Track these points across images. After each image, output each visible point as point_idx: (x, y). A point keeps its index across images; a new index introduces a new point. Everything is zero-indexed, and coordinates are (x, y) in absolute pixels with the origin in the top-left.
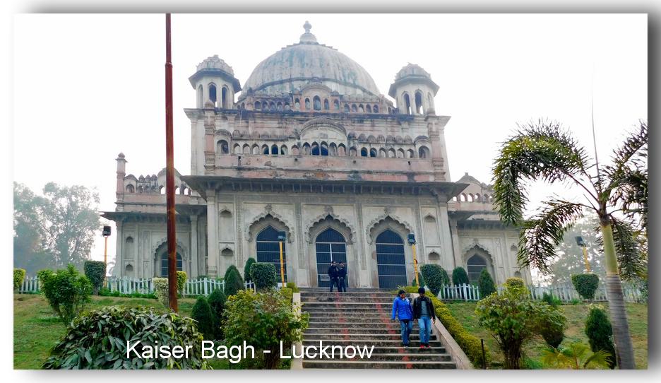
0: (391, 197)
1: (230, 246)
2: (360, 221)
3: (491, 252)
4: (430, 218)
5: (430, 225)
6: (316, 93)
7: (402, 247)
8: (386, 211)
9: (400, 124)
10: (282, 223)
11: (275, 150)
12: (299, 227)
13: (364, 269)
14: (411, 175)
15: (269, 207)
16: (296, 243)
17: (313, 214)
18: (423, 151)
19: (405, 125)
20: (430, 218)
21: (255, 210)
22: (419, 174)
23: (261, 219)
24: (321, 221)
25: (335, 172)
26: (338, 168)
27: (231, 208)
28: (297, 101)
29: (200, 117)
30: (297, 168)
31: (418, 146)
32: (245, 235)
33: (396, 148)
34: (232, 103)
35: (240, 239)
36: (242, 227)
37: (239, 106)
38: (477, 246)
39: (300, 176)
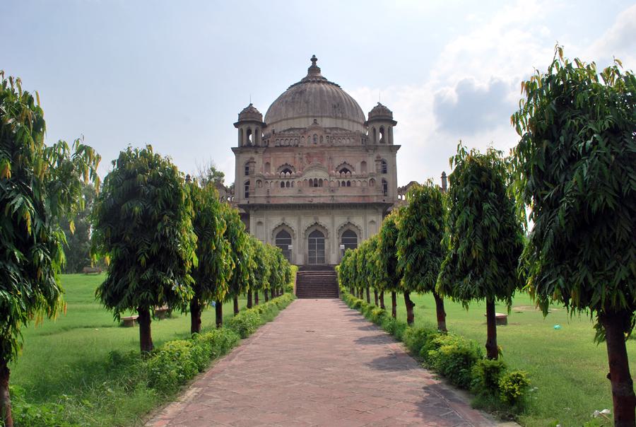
0: (352, 210)
2: (332, 224)
4: (372, 222)
5: (373, 226)
8: (348, 219)
10: (291, 228)
11: (288, 183)
12: (299, 230)
13: (333, 253)
15: (283, 219)
16: (297, 239)
17: (307, 221)
18: (372, 180)
19: (371, 152)
20: (372, 222)
22: (368, 196)
23: (279, 226)
26: (321, 196)
27: (263, 220)
29: (241, 153)
31: (370, 178)
32: (269, 237)
33: (356, 180)
36: (269, 231)
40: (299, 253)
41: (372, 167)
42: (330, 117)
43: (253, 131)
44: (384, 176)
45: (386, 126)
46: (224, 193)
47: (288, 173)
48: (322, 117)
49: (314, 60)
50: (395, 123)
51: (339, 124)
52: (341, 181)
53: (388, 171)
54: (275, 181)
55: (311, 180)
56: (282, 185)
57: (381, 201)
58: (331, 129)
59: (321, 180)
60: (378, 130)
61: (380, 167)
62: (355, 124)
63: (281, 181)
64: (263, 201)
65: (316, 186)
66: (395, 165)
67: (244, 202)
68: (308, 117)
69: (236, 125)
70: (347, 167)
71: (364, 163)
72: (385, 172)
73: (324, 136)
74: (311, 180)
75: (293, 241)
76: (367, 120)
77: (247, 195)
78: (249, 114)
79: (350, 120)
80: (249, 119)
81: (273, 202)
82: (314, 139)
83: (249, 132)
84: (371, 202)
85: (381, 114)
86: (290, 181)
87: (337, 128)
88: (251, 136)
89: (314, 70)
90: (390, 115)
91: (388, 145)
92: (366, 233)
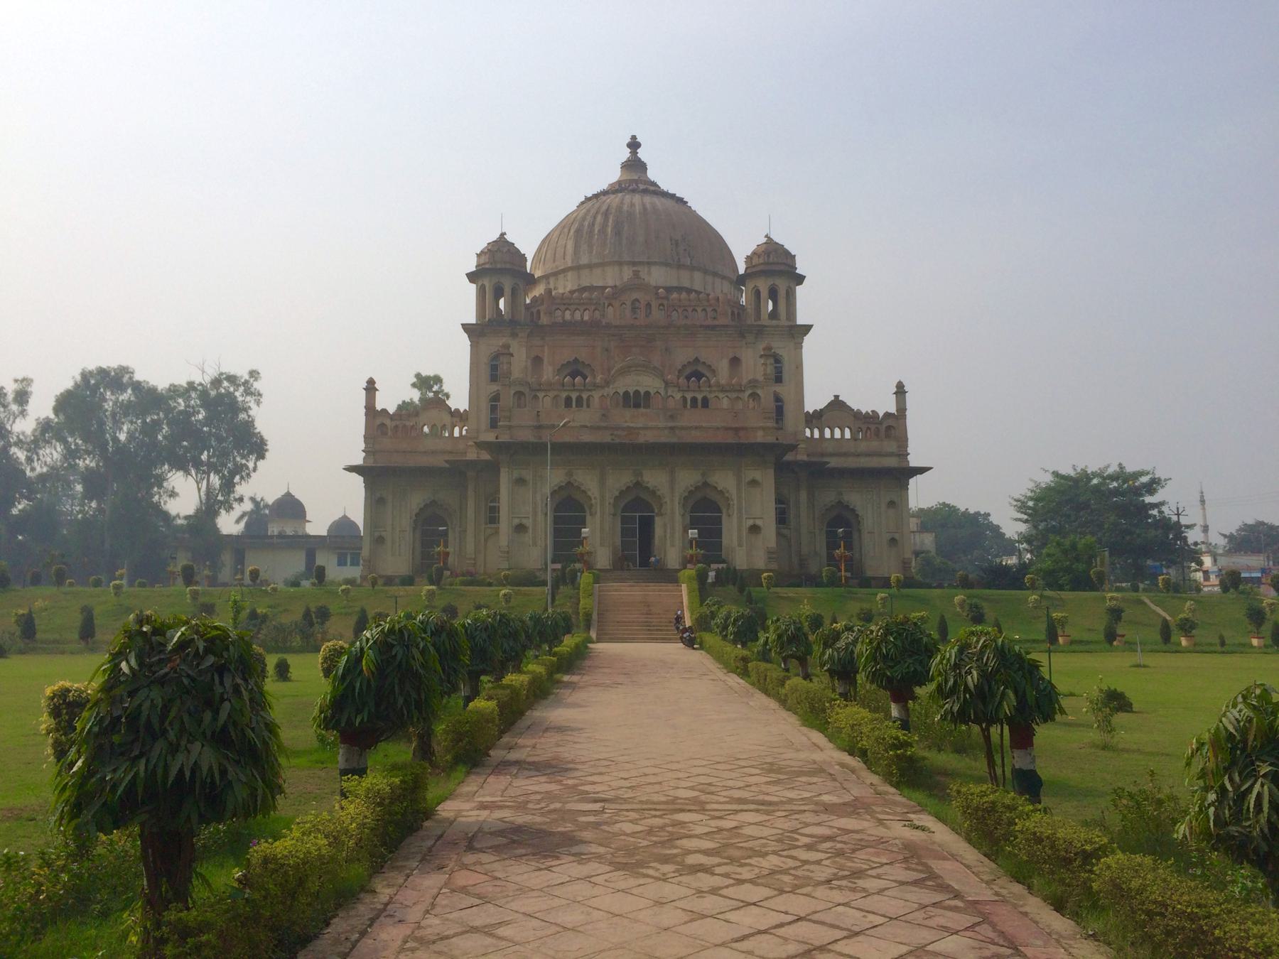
1: (524, 521)
2: (671, 486)
3: (860, 512)
4: (754, 483)
6: (635, 295)
7: (720, 517)
8: (703, 475)
10: (584, 492)
11: (579, 399)
14: (737, 430)
15: (570, 474)
17: (620, 480)
20: (754, 483)
21: (553, 477)
23: (561, 488)
24: (628, 488)
25: (645, 428)
26: (648, 426)
27: (528, 474)
28: (610, 305)
30: (603, 424)
33: (721, 395)
34: (523, 309)
35: (535, 513)
37: (532, 314)
38: (840, 502)
39: (606, 438)
40: (602, 545)
41: (753, 366)
42: (666, 264)
43: (507, 290)
44: (778, 388)
45: (782, 284)
46: (447, 419)
47: (578, 379)
49: (634, 145)
50: (800, 279)
52: (689, 396)
53: (786, 376)
54: (552, 394)
55: (626, 393)
56: (568, 402)
57: (770, 439)
58: (669, 290)
59: (647, 393)
60: (764, 293)
61: (770, 369)
62: (718, 281)
63: (564, 395)
64: (527, 436)
65: (637, 406)
66: (799, 367)
67: (490, 437)
68: (620, 264)
69: (472, 277)
70: (701, 369)
71: (735, 362)
72: (779, 379)
73: (654, 304)
74: (626, 393)
75: (588, 518)
76: (742, 269)
77: (494, 424)
79: (706, 272)
80: (499, 266)
81: (547, 437)
82: (634, 310)
83: (498, 293)
84: (752, 441)
86: (585, 396)
87: (679, 289)
88: (502, 302)
89: (634, 165)
91: (787, 323)
92: (740, 509)
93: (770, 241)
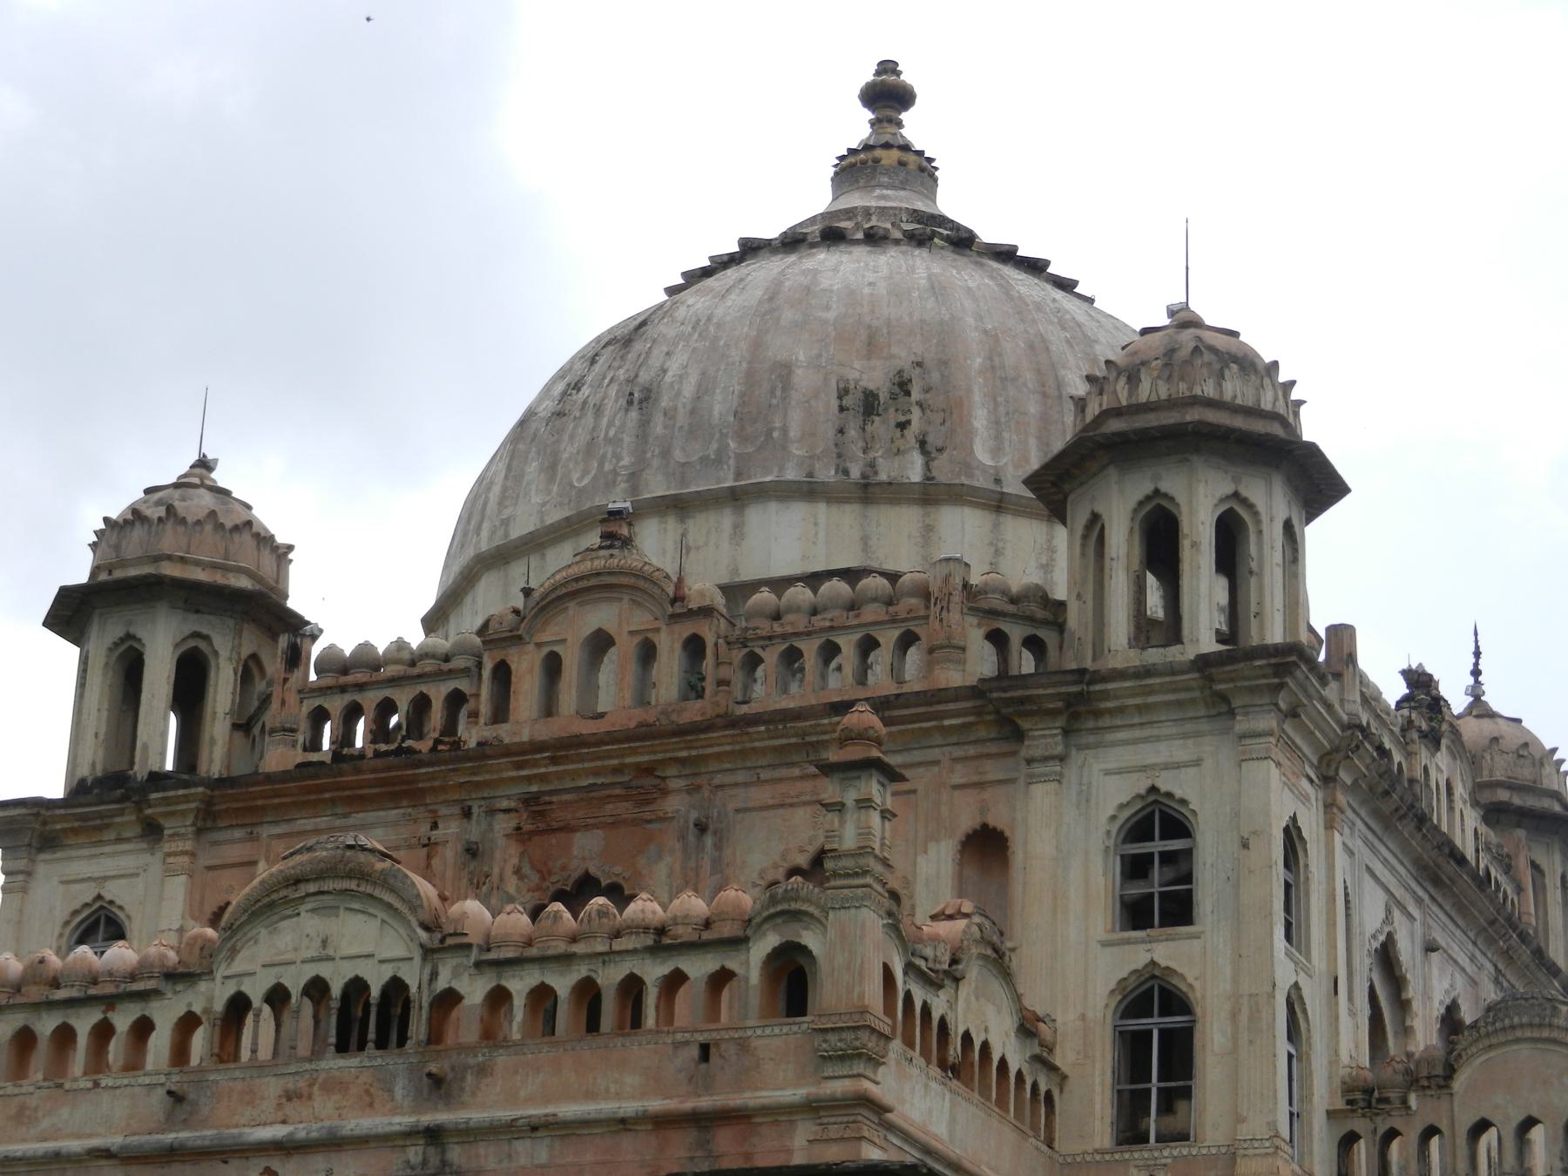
9: (1019, 736)
31: (764, 945)
42: (809, 491)
44: (1166, 950)
45: (1270, 500)
48: (737, 498)
49: (887, 95)
51: (897, 542)
78: (138, 533)
80: (132, 572)
85: (1144, 393)
90: (1234, 388)
93: (1184, 319)
